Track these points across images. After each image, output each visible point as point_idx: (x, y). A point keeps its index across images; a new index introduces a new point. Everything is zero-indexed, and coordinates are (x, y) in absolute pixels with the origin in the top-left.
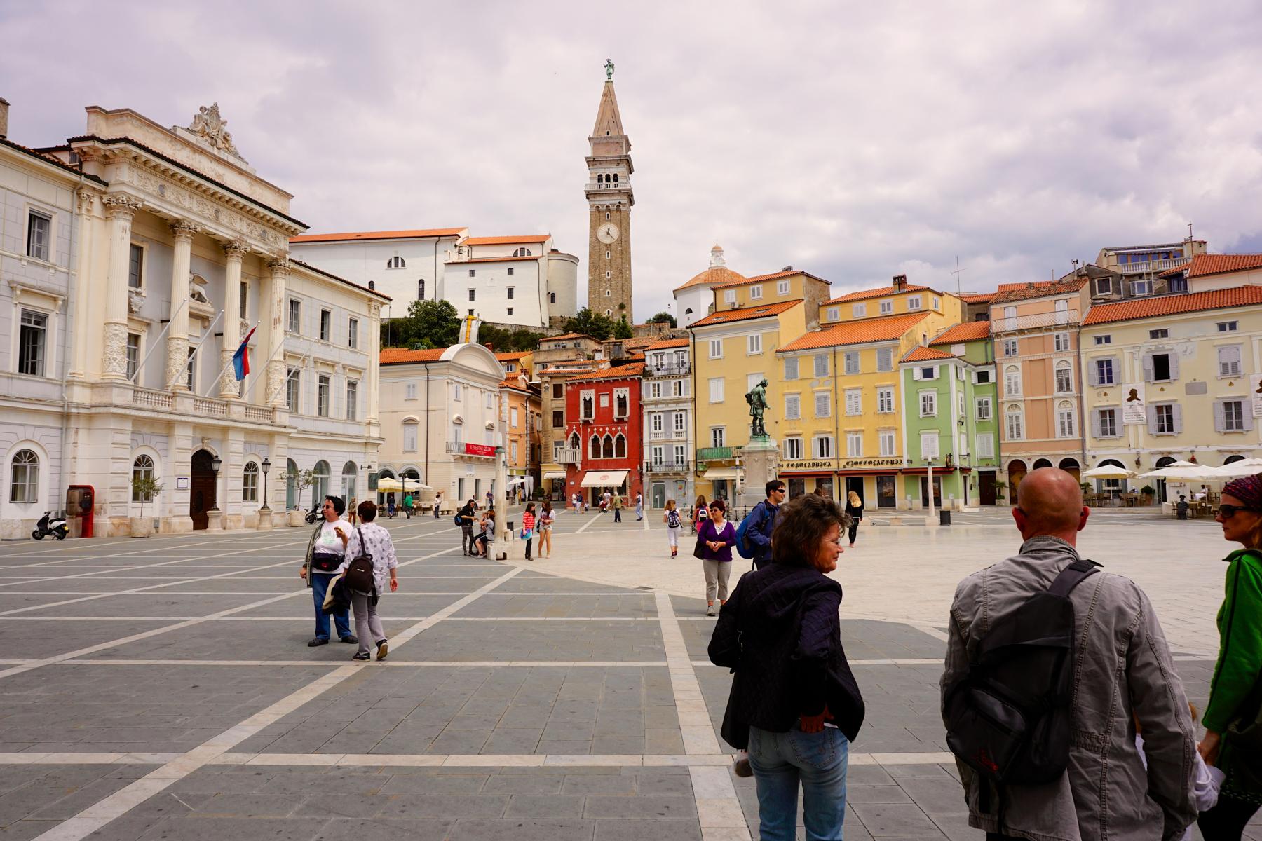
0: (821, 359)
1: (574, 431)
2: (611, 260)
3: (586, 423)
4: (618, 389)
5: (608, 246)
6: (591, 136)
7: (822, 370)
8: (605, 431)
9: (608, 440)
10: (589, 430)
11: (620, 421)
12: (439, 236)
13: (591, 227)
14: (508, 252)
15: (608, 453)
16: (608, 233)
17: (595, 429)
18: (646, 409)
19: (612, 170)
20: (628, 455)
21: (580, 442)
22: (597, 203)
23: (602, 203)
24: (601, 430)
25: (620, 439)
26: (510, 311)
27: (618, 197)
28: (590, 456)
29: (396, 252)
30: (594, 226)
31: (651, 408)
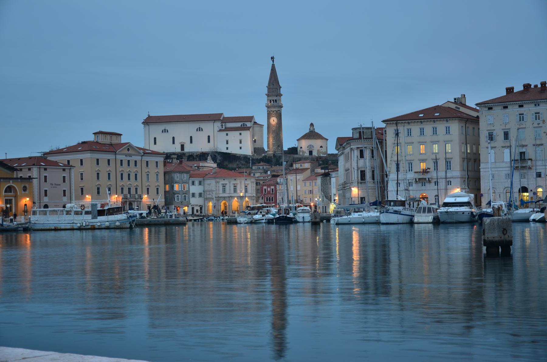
0: (310, 183)
2: (275, 130)
3: (265, 194)
7: (310, 185)
9: (270, 198)
11: (272, 194)
12: (215, 120)
14: (238, 125)
15: (270, 200)
18: (278, 191)
22: (269, 110)
25: (272, 198)
26: (241, 148)
28: (266, 201)
29: (199, 126)
30: (269, 119)
31: (279, 191)
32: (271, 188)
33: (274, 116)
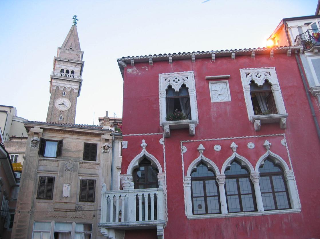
1: (144, 152)
4: (253, 71)
5: (61, 112)
6: (60, 46)
8: (226, 151)
10: (184, 149)
13: (51, 98)
16: (63, 104)
17: (201, 147)
19: (71, 68)
20: (302, 203)
21: (162, 177)
22: (58, 85)
23: (62, 85)
24: (217, 148)
27: (73, 84)
32: (245, 82)
33: (65, 97)
